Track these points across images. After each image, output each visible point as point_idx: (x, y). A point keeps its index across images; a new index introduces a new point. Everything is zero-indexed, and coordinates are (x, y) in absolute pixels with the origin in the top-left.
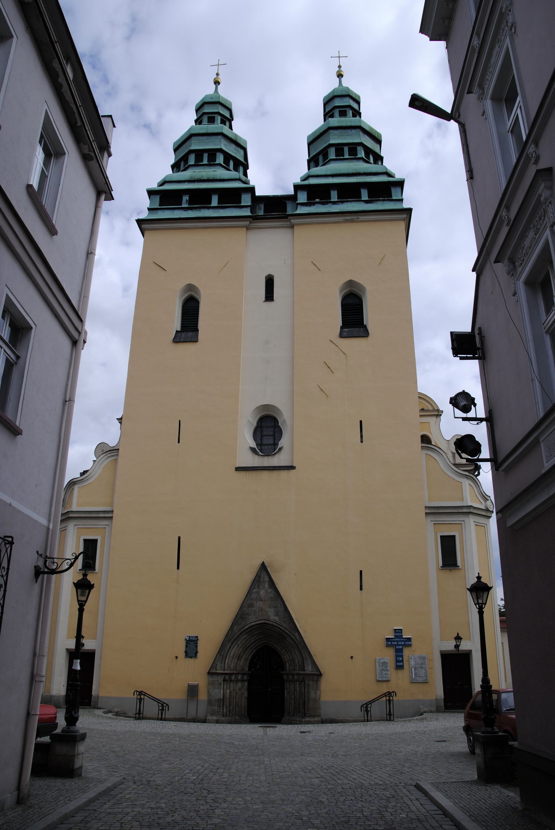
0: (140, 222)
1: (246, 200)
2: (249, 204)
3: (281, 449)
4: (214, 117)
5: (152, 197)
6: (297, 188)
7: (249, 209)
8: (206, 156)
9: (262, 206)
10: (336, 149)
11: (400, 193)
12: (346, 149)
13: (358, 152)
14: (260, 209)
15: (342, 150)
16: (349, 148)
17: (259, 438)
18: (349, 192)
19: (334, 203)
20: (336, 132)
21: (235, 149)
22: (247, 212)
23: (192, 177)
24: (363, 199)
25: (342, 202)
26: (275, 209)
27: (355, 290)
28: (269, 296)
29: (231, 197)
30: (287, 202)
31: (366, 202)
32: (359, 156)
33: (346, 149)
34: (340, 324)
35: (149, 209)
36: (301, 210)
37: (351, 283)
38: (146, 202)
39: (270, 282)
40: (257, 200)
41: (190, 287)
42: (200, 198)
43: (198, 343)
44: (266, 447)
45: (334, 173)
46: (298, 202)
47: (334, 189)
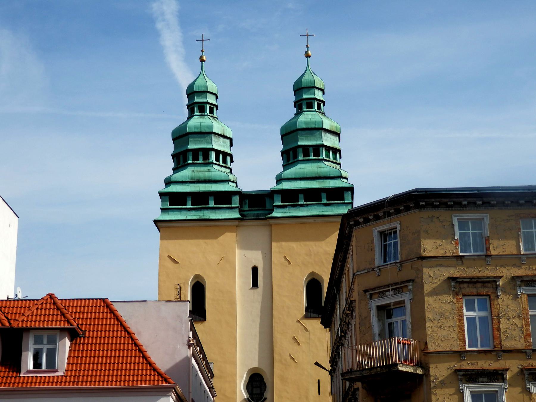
0: (156, 222)
1: (235, 202)
2: (238, 205)
3: (265, 399)
4: (204, 106)
7: (237, 210)
8: (201, 153)
9: (247, 201)
11: (350, 197)
12: (311, 149)
13: (321, 153)
14: (245, 204)
17: (250, 390)
18: (312, 196)
19: (302, 206)
20: (303, 132)
21: (223, 142)
23: (192, 178)
25: (307, 205)
27: (316, 278)
28: (255, 284)
29: (223, 199)
31: (326, 205)
33: (311, 149)
34: (305, 305)
35: (161, 209)
36: (276, 213)
37: (313, 273)
38: (158, 203)
39: (255, 270)
41: (197, 276)
42: (200, 200)
43: (206, 323)
44: (255, 396)
45: (301, 176)
46: (275, 204)
47: (301, 193)
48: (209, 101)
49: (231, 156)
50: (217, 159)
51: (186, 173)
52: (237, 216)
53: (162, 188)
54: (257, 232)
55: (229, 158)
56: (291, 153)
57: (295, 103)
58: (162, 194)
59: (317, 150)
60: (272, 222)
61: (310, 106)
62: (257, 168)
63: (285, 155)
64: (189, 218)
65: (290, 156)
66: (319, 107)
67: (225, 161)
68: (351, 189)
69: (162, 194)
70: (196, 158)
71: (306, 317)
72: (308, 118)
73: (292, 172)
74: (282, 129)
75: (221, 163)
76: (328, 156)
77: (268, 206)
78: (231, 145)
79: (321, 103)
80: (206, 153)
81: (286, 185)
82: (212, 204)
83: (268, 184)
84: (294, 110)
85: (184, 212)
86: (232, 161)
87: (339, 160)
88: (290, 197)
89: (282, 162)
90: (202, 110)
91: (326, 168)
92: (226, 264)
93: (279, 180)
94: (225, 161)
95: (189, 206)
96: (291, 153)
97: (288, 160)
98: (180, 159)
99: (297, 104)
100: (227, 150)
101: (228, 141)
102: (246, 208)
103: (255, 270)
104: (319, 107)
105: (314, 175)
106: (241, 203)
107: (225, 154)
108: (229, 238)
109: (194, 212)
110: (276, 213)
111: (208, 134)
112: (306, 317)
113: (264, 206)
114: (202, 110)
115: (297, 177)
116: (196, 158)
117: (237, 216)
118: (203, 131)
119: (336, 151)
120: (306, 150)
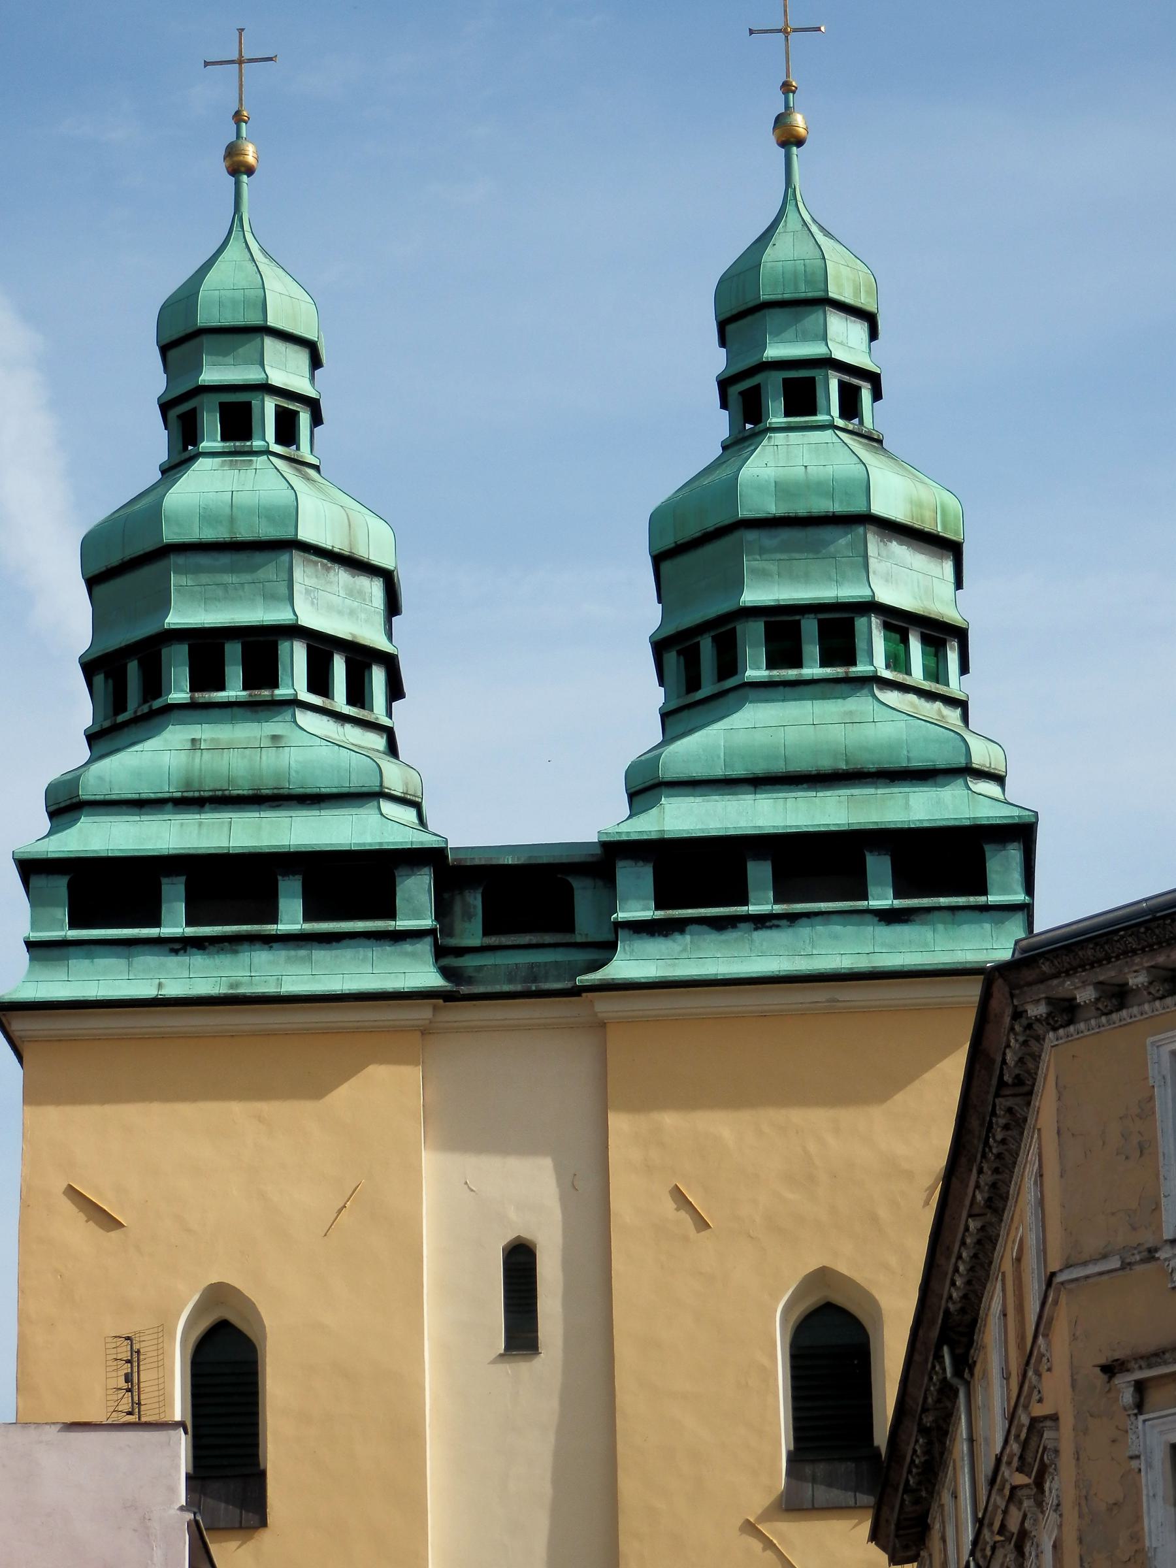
2: (427, 922)
4: (247, 406)
5: (35, 881)
6: (613, 854)
7: (425, 947)
8: (233, 651)
9: (475, 900)
10: (768, 625)
11: (1017, 876)
12: (810, 627)
13: (860, 644)
14: (468, 916)
15: (794, 633)
16: (821, 623)
18: (819, 868)
19: (761, 922)
22: (419, 972)
23: (188, 784)
24: (874, 903)
26: (526, 907)
27: (840, 1300)
28: (521, 1332)
29: (352, 888)
30: (570, 879)
31: (889, 917)
32: (861, 669)
33: (810, 627)
34: (784, 1443)
35: (31, 945)
36: (632, 963)
37: (822, 1276)
39: (520, 1263)
40: (451, 872)
41: (217, 1294)
42: (233, 891)
43: (265, 1538)
46: (622, 915)
47: (759, 857)
48: (277, 378)
49: (390, 663)
50: (319, 682)
51: (159, 757)
52: (427, 977)
53: (32, 833)
54: (528, 1058)
55: (378, 677)
56: (707, 647)
57: (724, 384)
58: (31, 869)
59: (838, 628)
60: (605, 1006)
61: (802, 401)
62: (527, 725)
63: (671, 658)
64: (173, 990)
65: (699, 662)
66: (850, 406)
67: (358, 694)
68: (1022, 834)
69: (31, 869)
70: (207, 675)
71: (792, 1505)
72: (793, 461)
73: (710, 744)
74: (657, 521)
75: (339, 701)
76: (898, 660)
77: (586, 925)
78: (393, 606)
79: (859, 385)
80: (261, 648)
81: (681, 817)
82: (291, 917)
83: (589, 813)
84: (720, 424)
85: (148, 960)
86: (395, 691)
87: (955, 685)
88: (700, 878)
89: (656, 696)
90: (238, 424)
91: (887, 723)
92: (373, 1224)
93: (645, 788)
94: (358, 694)
95: (174, 925)
96: (707, 647)
97: (693, 683)
98: (128, 683)
99: (734, 390)
100: (373, 636)
101: (375, 589)
102: (471, 934)
103: (520, 1263)
104: (850, 406)
105: (826, 764)
106: (442, 910)
107: (362, 658)
108: (386, 1092)
109: (198, 960)
110: (626, 965)
111: (272, 549)
112: (792, 1505)
113: (567, 923)
114: (238, 424)
115: (739, 771)
116: (207, 675)
117: (427, 977)
118: (244, 533)
119: (942, 635)
120: (782, 629)
